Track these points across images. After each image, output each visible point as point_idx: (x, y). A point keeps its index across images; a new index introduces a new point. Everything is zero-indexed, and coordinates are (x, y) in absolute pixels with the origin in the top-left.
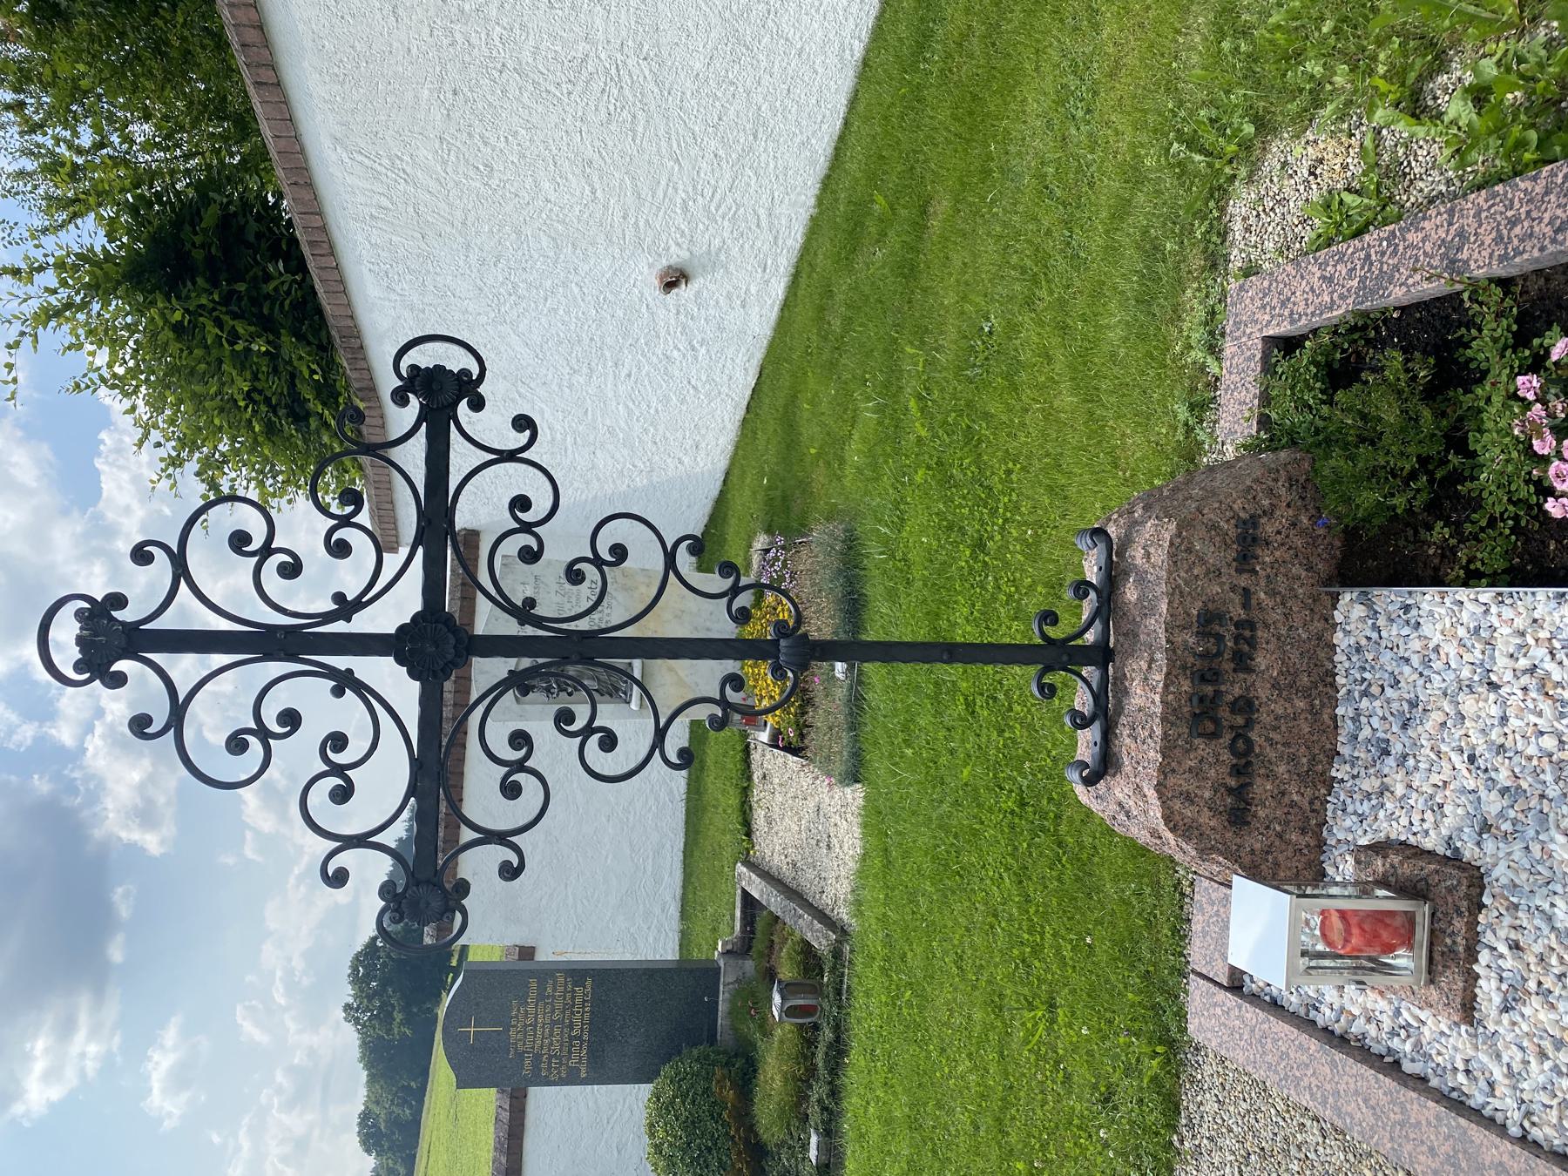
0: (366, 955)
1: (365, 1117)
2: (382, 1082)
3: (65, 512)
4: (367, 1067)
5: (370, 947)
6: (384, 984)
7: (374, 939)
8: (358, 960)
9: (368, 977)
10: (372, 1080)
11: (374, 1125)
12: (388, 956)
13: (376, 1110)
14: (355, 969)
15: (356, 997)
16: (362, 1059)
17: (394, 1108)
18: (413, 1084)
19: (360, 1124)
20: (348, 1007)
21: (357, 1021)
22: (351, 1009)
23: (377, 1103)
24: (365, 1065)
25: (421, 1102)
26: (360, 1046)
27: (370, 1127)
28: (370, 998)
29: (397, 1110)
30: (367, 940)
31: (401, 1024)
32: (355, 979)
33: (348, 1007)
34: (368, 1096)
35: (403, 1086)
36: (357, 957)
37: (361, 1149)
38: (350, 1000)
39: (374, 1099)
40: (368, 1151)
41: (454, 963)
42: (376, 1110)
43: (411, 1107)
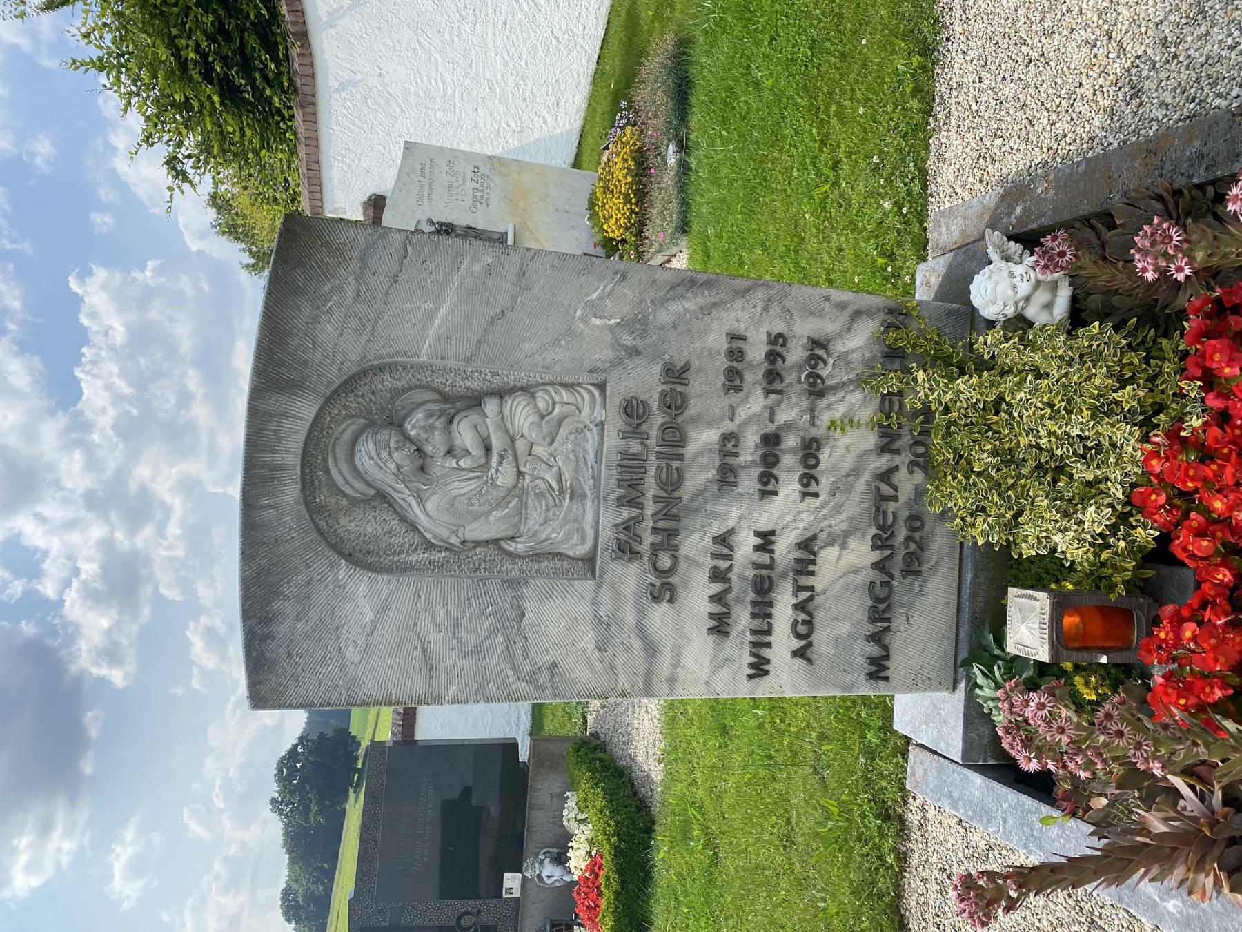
0: (289, 759)
1: (286, 893)
2: (300, 864)
3: (52, 413)
4: (290, 851)
5: (292, 754)
6: (303, 782)
7: (295, 746)
8: (281, 764)
9: (291, 776)
10: (293, 861)
11: (294, 900)
12: (307, 759)
13: (295, 886)
14: (280, 770)
15: (280, 792)
16: (284, 846)
17: (310, 885)
18: (325, 865)
20: (274, 801)
21: (281, 812)
22: (277, 802)
23: (296, 881)
24: (287, 850)
25: (332, 880)
27: (290, 901)
28: (292, 793)
31: (317, 814)
32: (283, 780)
33: (274, 801)
34: (289, 876)
36: (281, 762)
37: (282, 919)
38: (276, 795)
39: (294, 879)
40: (289, 921)
41: (359, 766)
42: (295, 886)
43: (323, 884)
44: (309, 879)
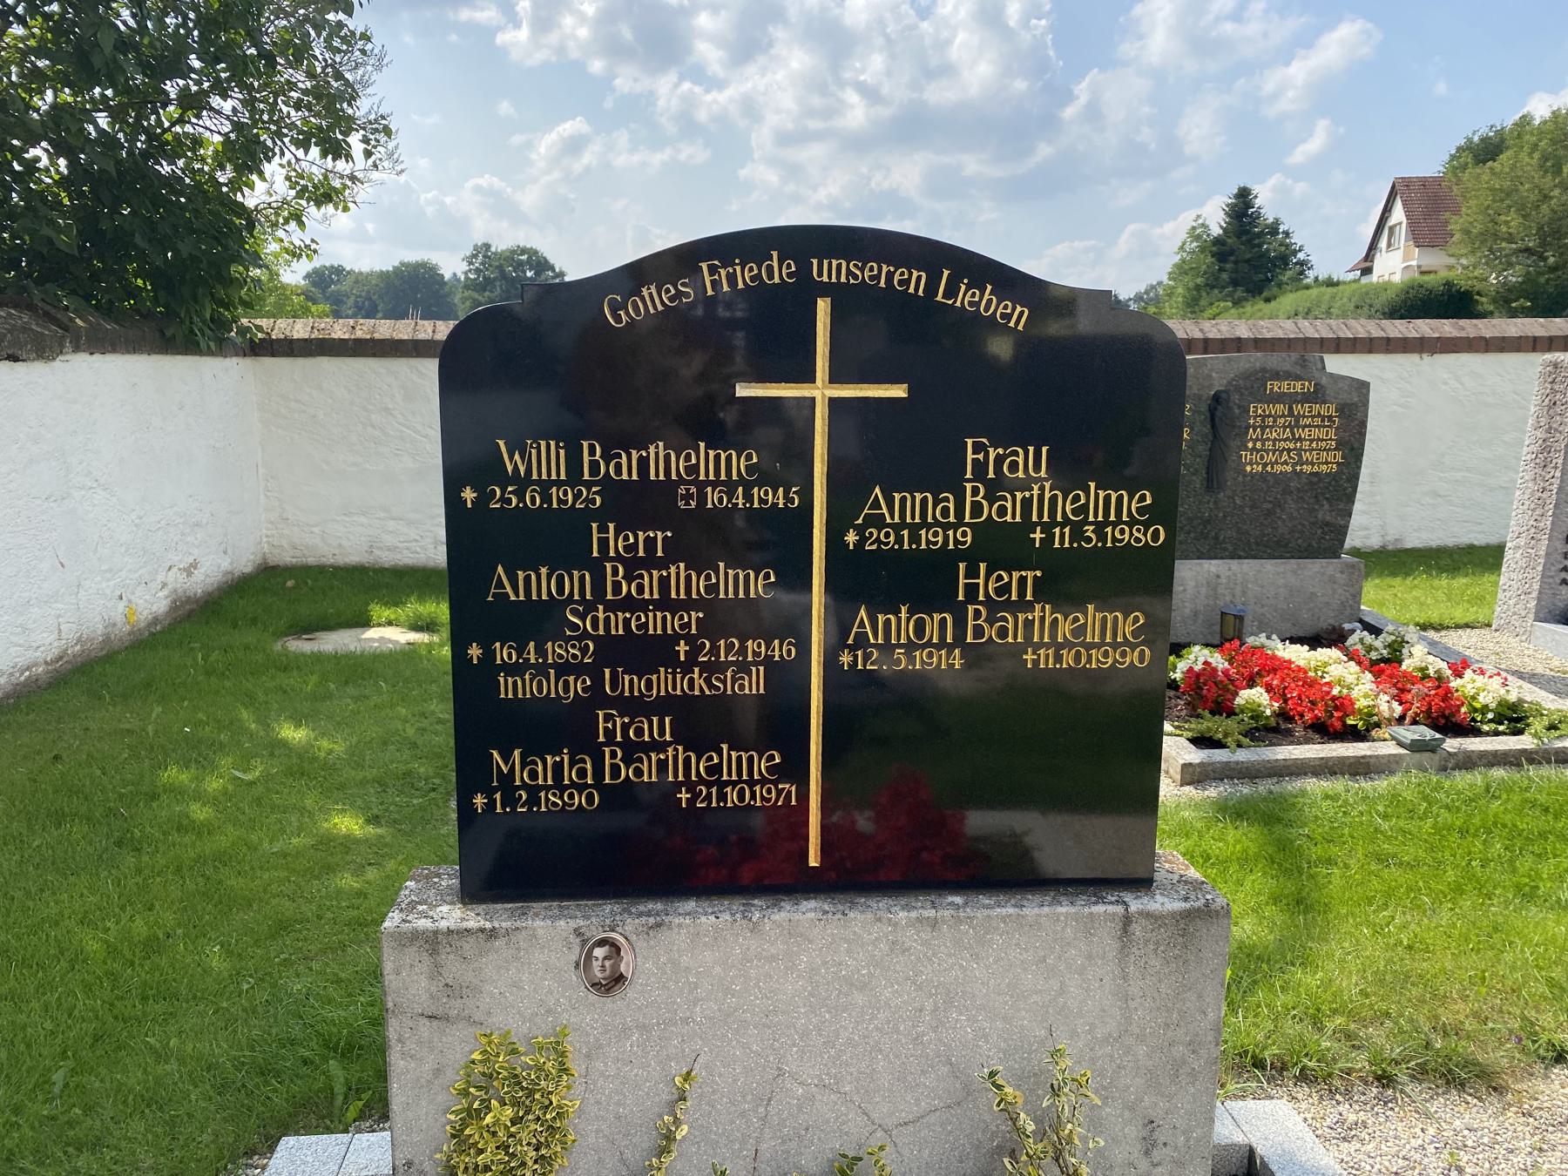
1: (338, 270)
5: (542, 265)
7: (552, 268)
8: (532, 253)
9: (519, 266)
10: (383, 276)
11: (332, 281)
14: (524, 251)
15: (495, 254)
16: (403, 264)
17: (353, 298)
19: (332, 267)
20: (487, 246)
21: (475, 256)
23: (356, 282)
26: (417, 262)
27: (330, 277)
28: (500, 268)
29: (351, 302)
30: (552, 262)
33: (487, 246)
34: (361, 273)
35: (376, 306)
36: (536, 252)
38: (493, 249)
39: (360, 279)
40: (308, 276)
42: (350, 280)
44: (360, 296)
